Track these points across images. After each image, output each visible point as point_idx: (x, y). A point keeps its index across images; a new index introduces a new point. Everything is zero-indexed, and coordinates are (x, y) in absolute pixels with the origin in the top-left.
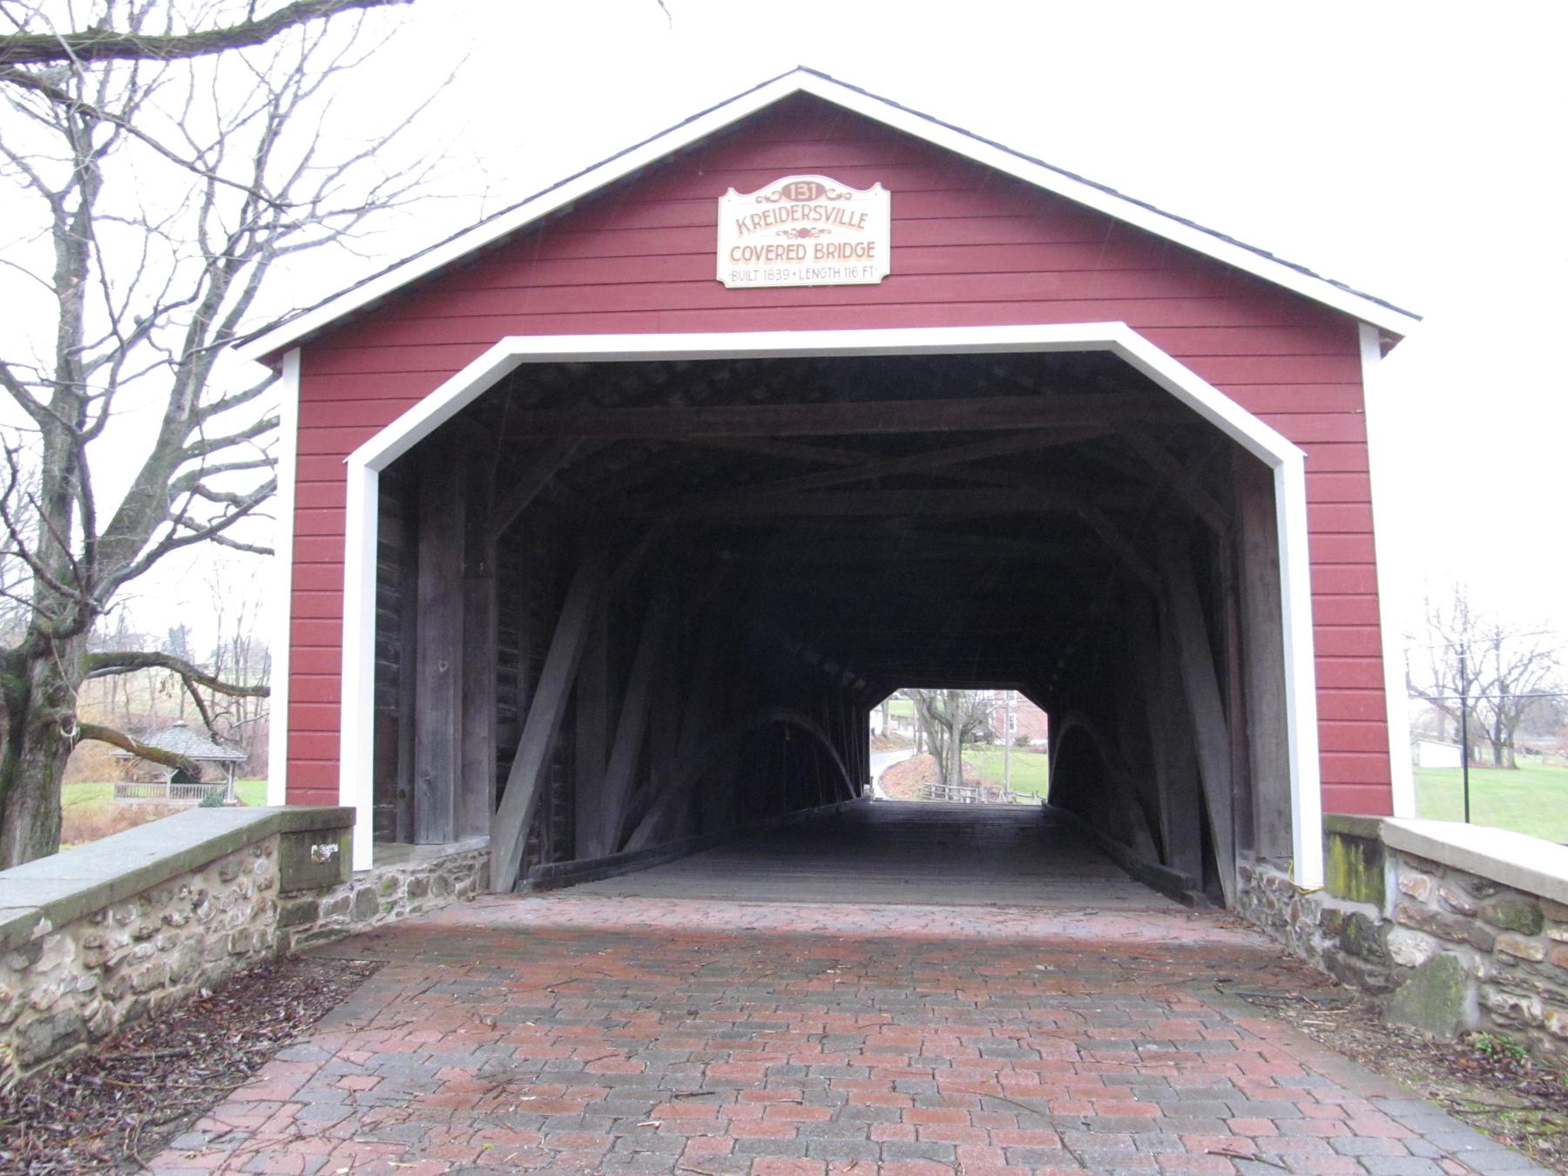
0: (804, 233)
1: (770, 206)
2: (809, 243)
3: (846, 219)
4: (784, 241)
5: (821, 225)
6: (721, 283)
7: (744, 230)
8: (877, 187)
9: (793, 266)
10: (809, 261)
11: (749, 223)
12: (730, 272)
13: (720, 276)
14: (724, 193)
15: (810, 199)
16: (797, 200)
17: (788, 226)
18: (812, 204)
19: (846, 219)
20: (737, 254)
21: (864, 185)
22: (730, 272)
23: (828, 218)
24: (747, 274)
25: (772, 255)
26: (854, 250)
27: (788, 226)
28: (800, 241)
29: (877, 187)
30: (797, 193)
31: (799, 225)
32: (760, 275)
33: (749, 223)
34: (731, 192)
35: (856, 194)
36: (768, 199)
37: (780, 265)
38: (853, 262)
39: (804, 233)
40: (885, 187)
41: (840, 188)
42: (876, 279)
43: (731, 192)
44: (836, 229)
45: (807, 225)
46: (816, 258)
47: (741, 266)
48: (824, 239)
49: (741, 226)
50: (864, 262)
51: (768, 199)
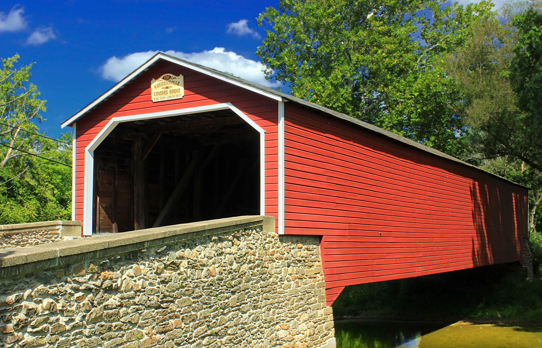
0: (167, 88)
2: (168, 90)
4: (163, 90)
5: (170, 85)
6: (152, 101)
8: (181, 75)
9: (166, 96)
10: (169, 94)
12: (154, 98)
13: (152, 99)
14: (152, 80)
17: (164, 86)
21: (178, 75)
22: (154, 98)
27: (164, 86)
28: (166, 90)
29: (181, 75)
32: (161, 98)
34: (153, 79)
35: (177, 77)
37: (163, 96)
38: (177, 94)
39: (167, 88)
40: (182, 75)
41: (174, 76)
42: (181, 97)
47: (156, 97)
48: (171, 89)
49: (155, 87)
50: (178, 94)
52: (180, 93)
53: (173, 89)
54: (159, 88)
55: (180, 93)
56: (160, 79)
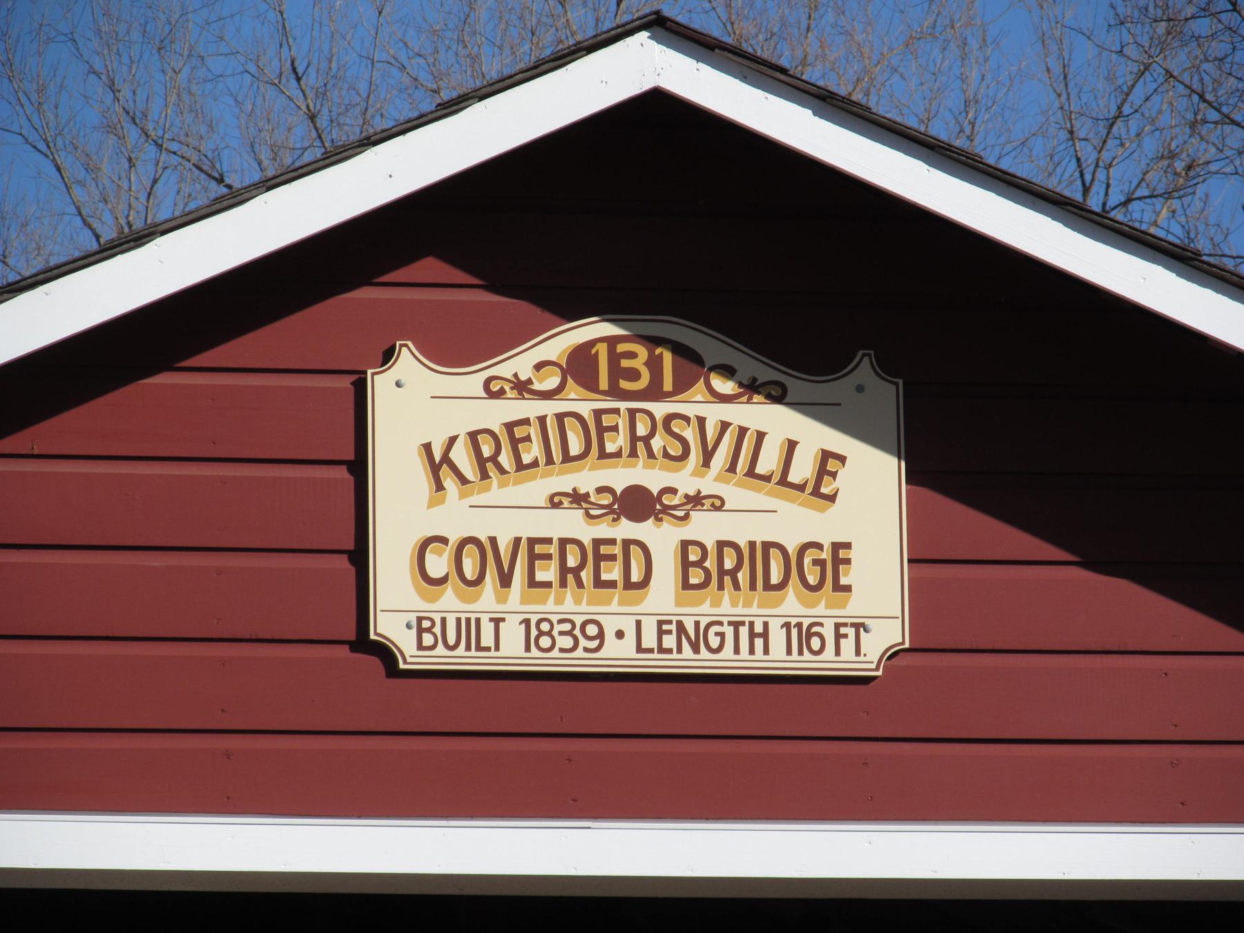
1: (531, 408)
3: (769, 462)
4: (571, 524)
5: (686, 480)
6: (384, 653)
7: (450, 483)
8: (864, 371)
11: (462, 456)
15: (654, 392)
16: (615, 392)
17: (587, 479)
18: (660, 409)
19: (769, 462)
20: (438, 564)
23: (707, 457)
24: (469, 630)
25: (546, 573)
26: (794, 563)
27: (587, 479)
28: (626, 529)
29: (864, 371)
30: (617, 372)
31: (620, 477)
33: (462, 456)
34: (407, 362)
36: (522, 388)
38: (792, 604)
40: (886, 368)
43: (407, 362)
44: (736, 494)
45: (653, 478)
46: (686, 585)
47: (450, 602)
50: (823, 611)
51: (522, 388)
52: (855, 607)
53: (743, 530)
54: (496, 492)
55: (855, 607)
56: (520, 363)
